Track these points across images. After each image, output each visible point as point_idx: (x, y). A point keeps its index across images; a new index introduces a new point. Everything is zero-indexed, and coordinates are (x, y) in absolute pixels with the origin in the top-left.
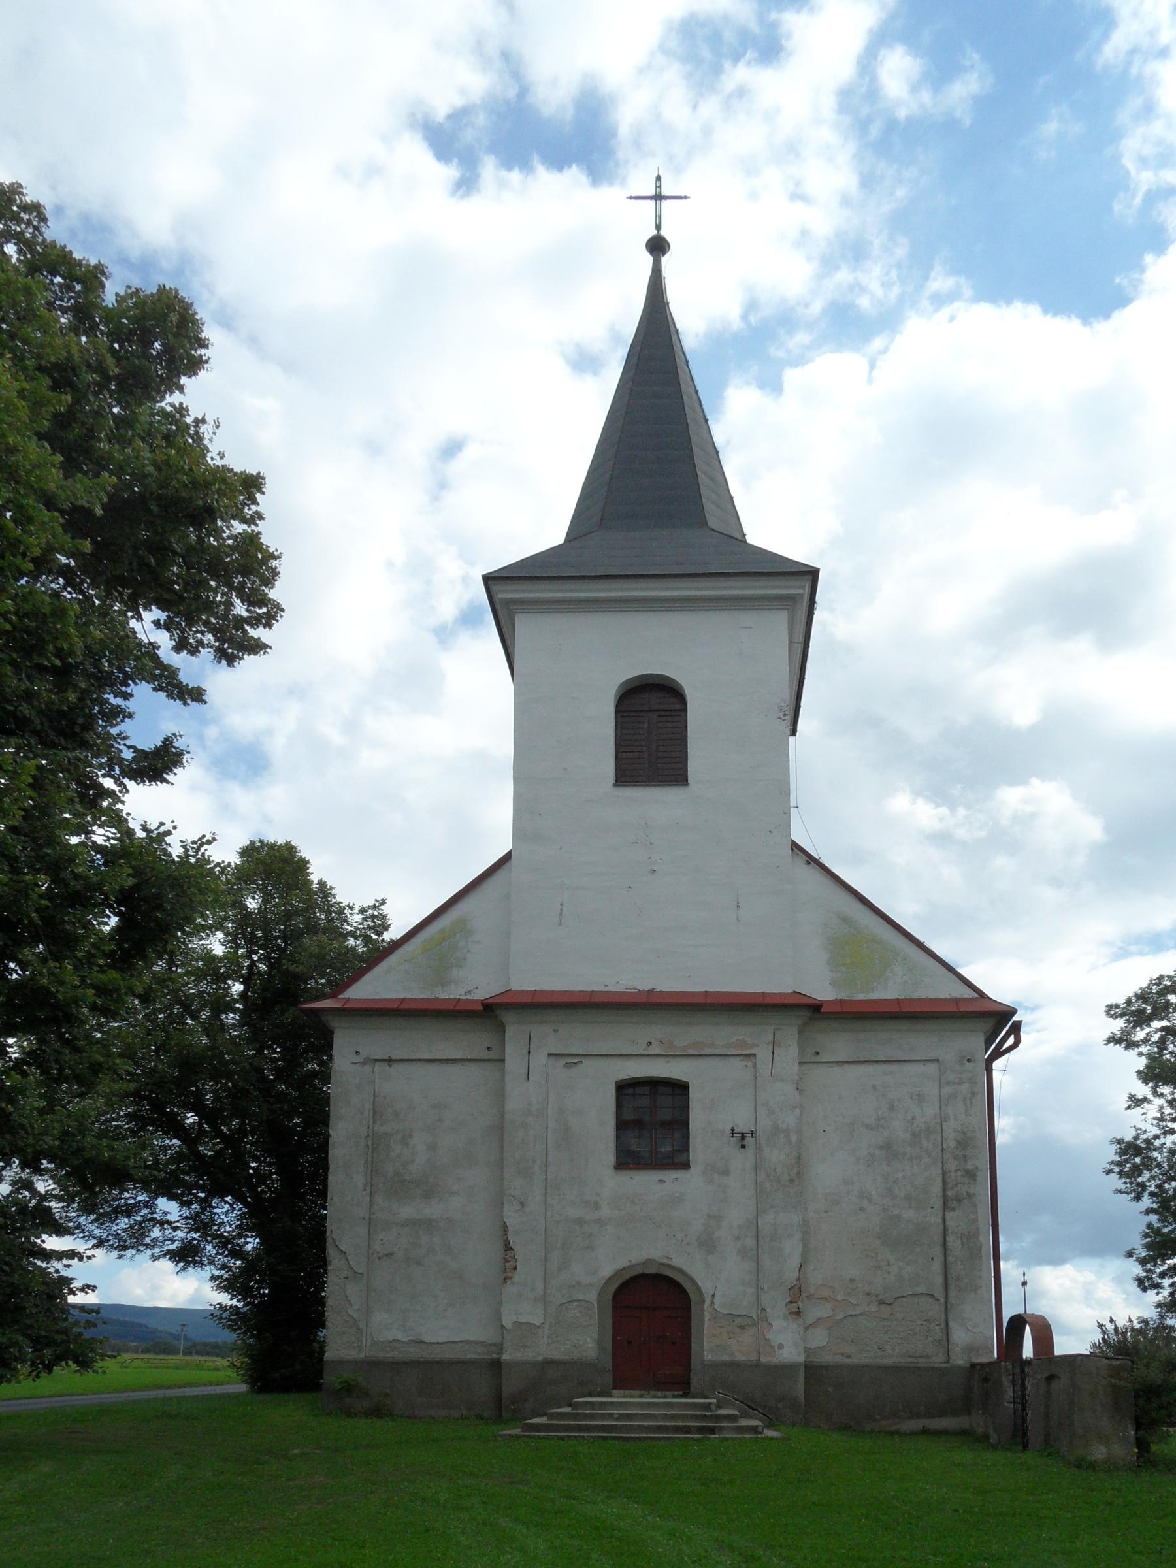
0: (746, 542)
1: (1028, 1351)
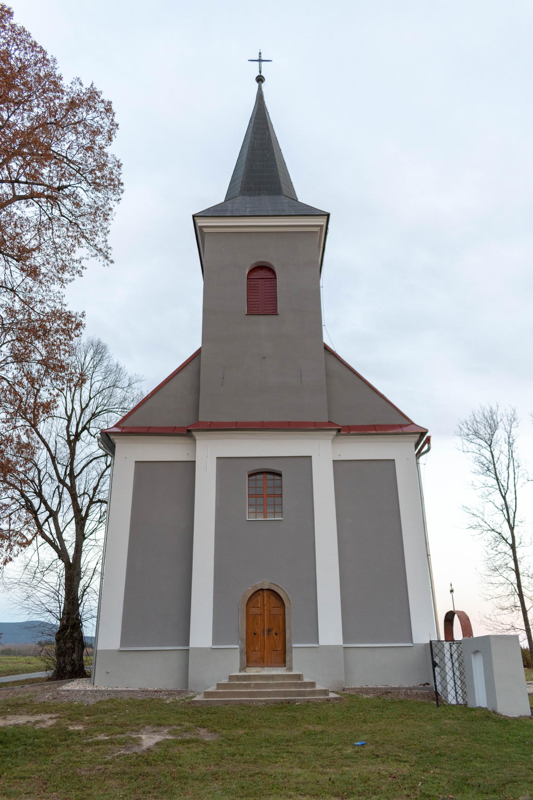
0: (297, 201)
1: (458, 634)
